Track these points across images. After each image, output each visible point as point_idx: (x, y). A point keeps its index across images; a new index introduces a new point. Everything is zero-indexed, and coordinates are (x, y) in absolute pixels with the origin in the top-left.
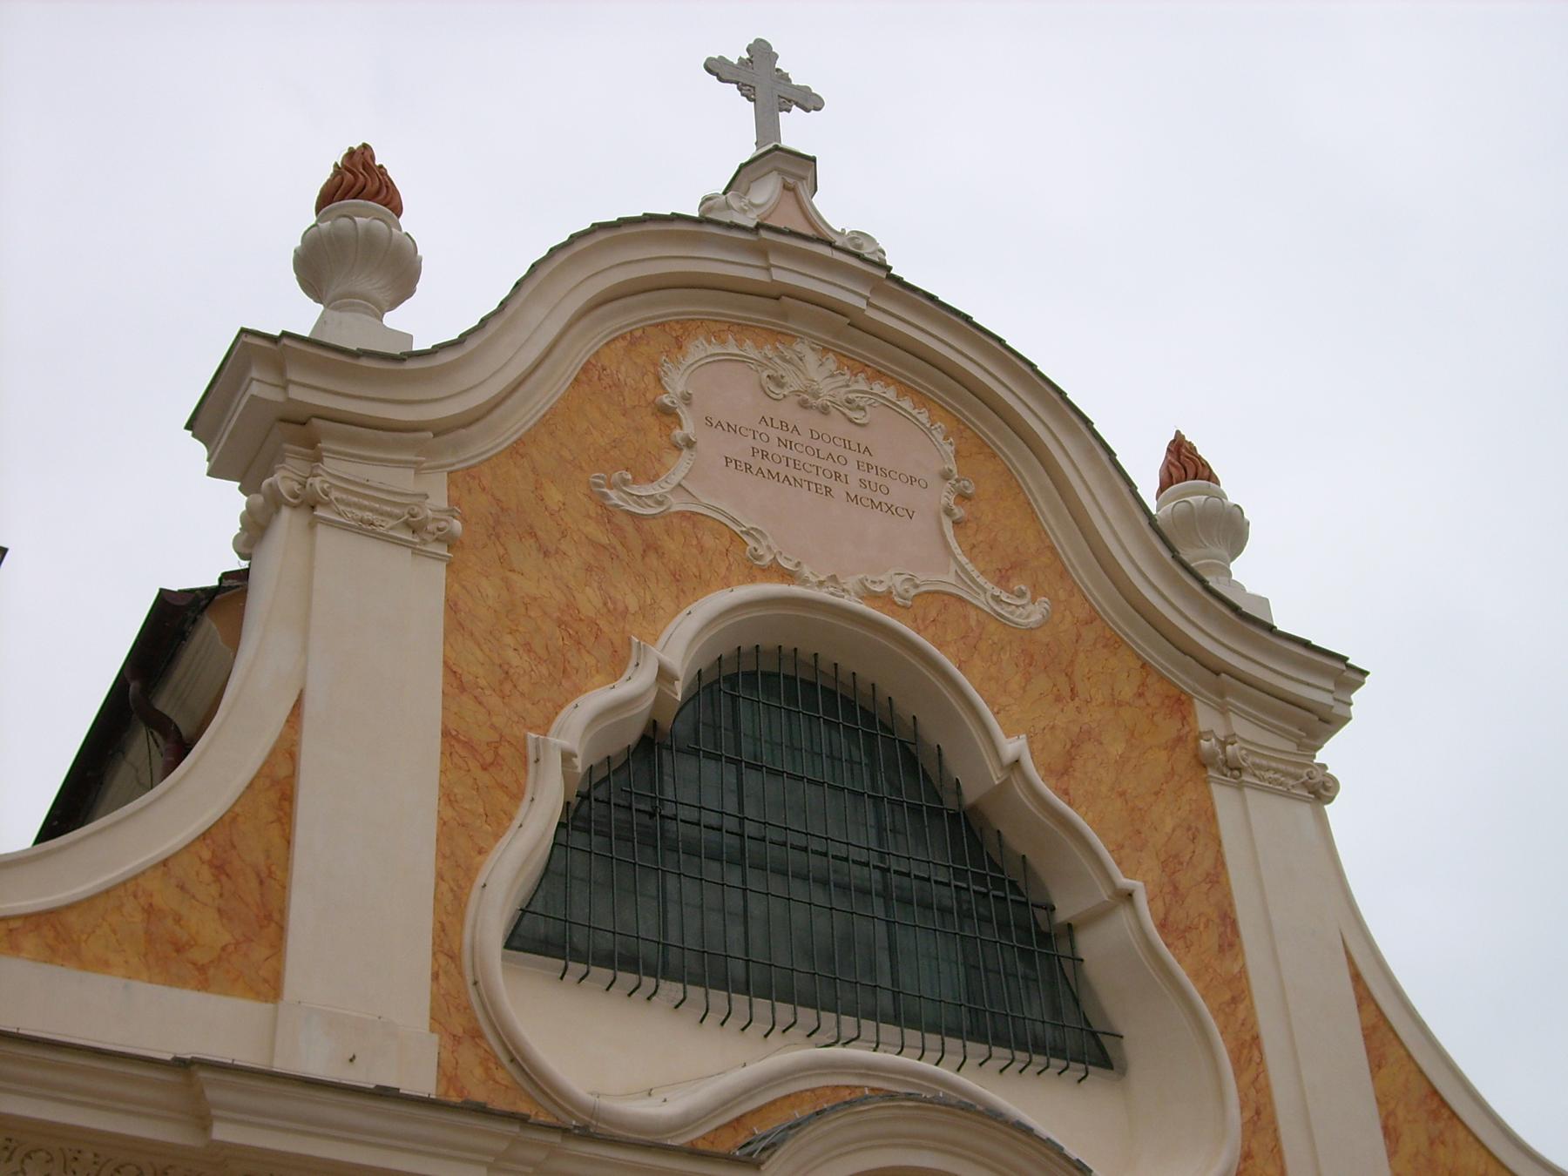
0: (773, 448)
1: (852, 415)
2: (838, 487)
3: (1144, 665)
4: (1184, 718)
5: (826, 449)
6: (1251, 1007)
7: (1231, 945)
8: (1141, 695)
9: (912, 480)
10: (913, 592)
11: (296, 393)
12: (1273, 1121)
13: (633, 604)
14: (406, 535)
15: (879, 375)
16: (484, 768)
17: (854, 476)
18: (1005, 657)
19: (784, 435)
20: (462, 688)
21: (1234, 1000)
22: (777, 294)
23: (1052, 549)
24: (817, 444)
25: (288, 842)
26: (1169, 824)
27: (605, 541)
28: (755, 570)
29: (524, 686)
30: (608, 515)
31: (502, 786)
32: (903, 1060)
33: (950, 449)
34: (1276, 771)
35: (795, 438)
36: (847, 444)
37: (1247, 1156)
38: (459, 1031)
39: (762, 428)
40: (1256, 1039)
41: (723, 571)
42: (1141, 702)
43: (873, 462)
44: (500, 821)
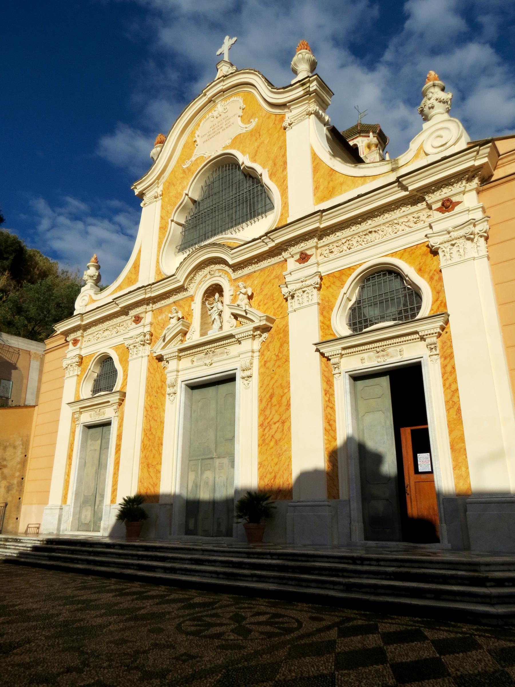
5: (219, 124)
10: (230, 141)
14: (155, 200)
21: (284, 181)
22: (210, 101)
26: (276, 150)
30: (184, 172)
33: (241, 101)
36: (224, 119)
37: (282, 215)
40: (287, 187)
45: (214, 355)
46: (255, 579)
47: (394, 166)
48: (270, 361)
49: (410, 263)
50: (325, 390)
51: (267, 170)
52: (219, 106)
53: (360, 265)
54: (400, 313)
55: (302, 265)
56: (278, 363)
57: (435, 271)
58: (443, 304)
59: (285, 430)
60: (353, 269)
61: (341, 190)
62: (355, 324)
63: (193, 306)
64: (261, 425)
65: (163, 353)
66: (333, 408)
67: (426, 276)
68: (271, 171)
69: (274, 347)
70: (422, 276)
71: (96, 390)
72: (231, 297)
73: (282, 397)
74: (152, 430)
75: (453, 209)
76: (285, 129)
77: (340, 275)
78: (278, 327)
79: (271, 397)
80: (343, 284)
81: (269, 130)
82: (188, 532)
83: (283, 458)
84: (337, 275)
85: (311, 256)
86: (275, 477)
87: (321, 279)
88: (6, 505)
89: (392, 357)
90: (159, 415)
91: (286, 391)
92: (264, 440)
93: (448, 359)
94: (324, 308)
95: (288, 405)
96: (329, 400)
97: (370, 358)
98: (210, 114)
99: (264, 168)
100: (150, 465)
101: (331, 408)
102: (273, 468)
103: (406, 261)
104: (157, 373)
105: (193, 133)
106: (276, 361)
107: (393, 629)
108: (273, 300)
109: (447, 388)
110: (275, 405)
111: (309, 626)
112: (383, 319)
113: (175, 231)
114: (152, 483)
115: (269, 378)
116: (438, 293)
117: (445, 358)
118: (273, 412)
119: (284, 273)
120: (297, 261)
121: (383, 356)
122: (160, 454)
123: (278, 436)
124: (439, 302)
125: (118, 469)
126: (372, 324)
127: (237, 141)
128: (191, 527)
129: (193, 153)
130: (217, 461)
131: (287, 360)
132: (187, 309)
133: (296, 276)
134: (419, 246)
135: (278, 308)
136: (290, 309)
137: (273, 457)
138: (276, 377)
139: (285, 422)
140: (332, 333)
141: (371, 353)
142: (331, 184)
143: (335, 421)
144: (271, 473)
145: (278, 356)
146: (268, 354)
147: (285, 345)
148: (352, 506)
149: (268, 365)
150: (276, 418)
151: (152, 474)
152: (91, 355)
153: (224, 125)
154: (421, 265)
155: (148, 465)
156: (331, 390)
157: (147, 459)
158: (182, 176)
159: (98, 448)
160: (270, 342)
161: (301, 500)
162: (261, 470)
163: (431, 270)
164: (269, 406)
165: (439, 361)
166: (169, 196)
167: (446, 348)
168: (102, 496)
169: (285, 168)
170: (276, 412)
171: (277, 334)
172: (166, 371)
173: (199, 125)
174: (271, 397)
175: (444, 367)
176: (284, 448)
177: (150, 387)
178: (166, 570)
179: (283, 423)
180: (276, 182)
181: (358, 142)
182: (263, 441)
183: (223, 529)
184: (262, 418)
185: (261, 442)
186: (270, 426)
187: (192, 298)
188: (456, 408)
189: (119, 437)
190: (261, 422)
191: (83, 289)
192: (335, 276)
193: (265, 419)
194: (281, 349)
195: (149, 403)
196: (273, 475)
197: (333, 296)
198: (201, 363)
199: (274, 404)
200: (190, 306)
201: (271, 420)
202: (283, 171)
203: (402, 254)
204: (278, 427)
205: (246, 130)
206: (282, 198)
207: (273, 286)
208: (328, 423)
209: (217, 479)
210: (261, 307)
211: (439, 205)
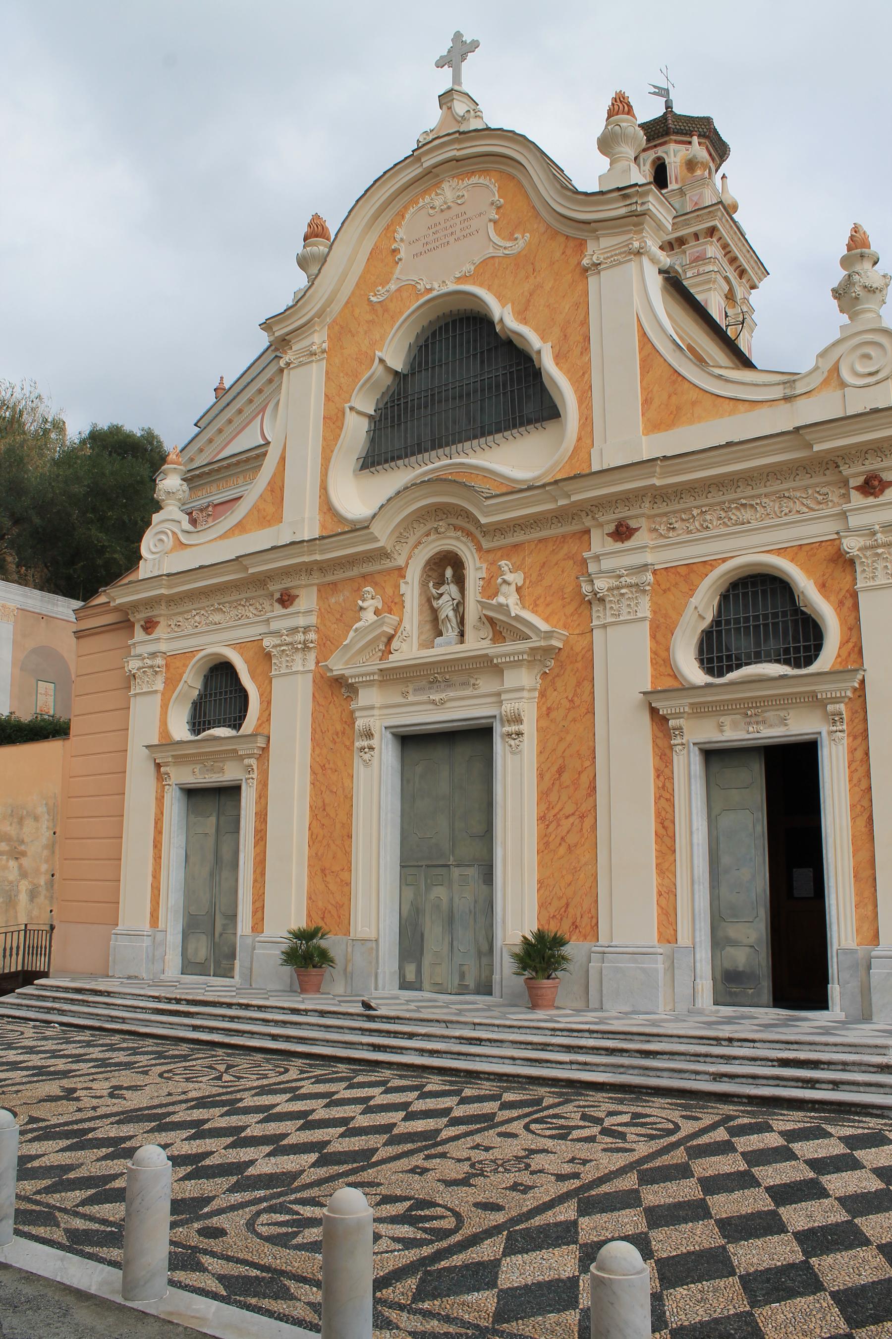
1: (459, 202)
2: (451, 239)
3: (567, 236)
5: (448, 224)
10: (473, 268)
11: (277, 334)
15: (473, 173)
19: (434, 230)
21: (584, 374)
26: (567, 307)
28: (419, 295)
32: (453, 461)
33: (495, 190)
34: (616, 255)
36: (457, 216)
37: (579, 439)
45: (449, 686)
46: (574, 1067)
49: (809, 572)
51: (550, 344)
52: (445, 185)
53: (724, 560)
54: (787, 651)
55: (619, 546)
58: (856, 649)
59: (584, 830)
60: (711, 565)
62: (710, 660)
63: (403, 588)
64: (542, 818)
65: (347, 673)
66: (671, 801)
67: (832, 598)
68: (557, 348)
69: (566, 685)
70: (827, 597)
71: (199, 723)
72: (481, 583)
73: (580, 773)
75: (882, 491)
76: (586, 270)
77: (687, 575)
78: (572, 649)
79: (560, 771)
80: (692, 591)
81: (552, 264)
82: (404, 985)
83: (582, 875)
85: (637, 530)
86: (567, 905)
87: (655, 572)
88: (52, 928)
89: (771, 726)
91: (587, 763)
92: (547, 844)
94: (658, 627)
95: (593, 789)
96: (664, 786)
97: (735, 725)
98: (427, 199)
99: (543, 338)
100: (327, 872)
102: (563, 890)
103: (802, 567)
105: (389, 231)
106: (569, 709)
107: (790, 1126)
109: (855, 785)
110: (567, 787)
111: (688, 1127)
112: (758, 658)
113: (356, 430)
114: (334, 903)
116: (850, 629)
117: (855, 738)
118: (564, 797)
119: (586, 555)
120: (608, 535)
121: (757, 723)
122: (348, 854)
123: (571, 839)
124: (850, 645)
125: (263, 874)
126: (739, 666)
127: (486, 270)
128: (411, 976)
129: (392, 273)
130: (456, 872)
131: (591, 711)
132: (389, 591)
133: (607, 564)
134: (823, 544)
135: (572, 615)
136: (595, 623)
137: (564, 872)
138: (569, 738)
139: (587, 815)
140: (672, 674)
141: (738, 716)
142: (674, 398)
144: (560, 898)
145: (572, 701)
146: (553, 697)
148: (698, 957)
149: (553, 715)
150: (569, 808)
151: (332, 887)
152: (189, 655)
154: (825, 577)
155: (323, 871)
156: (667, 771)
157: (320, 860)
158: (369, 317)
159: (212, 831)
161: (613, 944)
162: (542, 892)
164: (556, 787)
165: (845, 741)
167: (856, 721)
168: (232, 917)
169: (586, 349)
171: (571, 663)
172: (353, 706)
173: (403, 217)
174: (560, 771)
175: (852, 751)
177: (318, 730)
178: (422, 1051)
179: (582, 817)
180: (570, 373)
181: (666, 153)
182: (545, 845)
183: (470, 981)
184: (544, 807)
186: (558, 821)
187: (401, 572)
188: (866, 816)
189: (262, 816)
190: (542, 814)
191: (156, 518)
192: (679, 574)
193: (548, 809)
194: (579, 691)
196: (564, 901)
198: (424, 698)
199: (565, 785)
200: (397, 587)
201: (561, 810)
202: (582, 353)
203: (795, 552)
205: (507, 252)
206: (579, 407)
207: (563, 571)
208: (662, 823)
209: (456, 899)
210: (540, 609)
211: (860, 481)
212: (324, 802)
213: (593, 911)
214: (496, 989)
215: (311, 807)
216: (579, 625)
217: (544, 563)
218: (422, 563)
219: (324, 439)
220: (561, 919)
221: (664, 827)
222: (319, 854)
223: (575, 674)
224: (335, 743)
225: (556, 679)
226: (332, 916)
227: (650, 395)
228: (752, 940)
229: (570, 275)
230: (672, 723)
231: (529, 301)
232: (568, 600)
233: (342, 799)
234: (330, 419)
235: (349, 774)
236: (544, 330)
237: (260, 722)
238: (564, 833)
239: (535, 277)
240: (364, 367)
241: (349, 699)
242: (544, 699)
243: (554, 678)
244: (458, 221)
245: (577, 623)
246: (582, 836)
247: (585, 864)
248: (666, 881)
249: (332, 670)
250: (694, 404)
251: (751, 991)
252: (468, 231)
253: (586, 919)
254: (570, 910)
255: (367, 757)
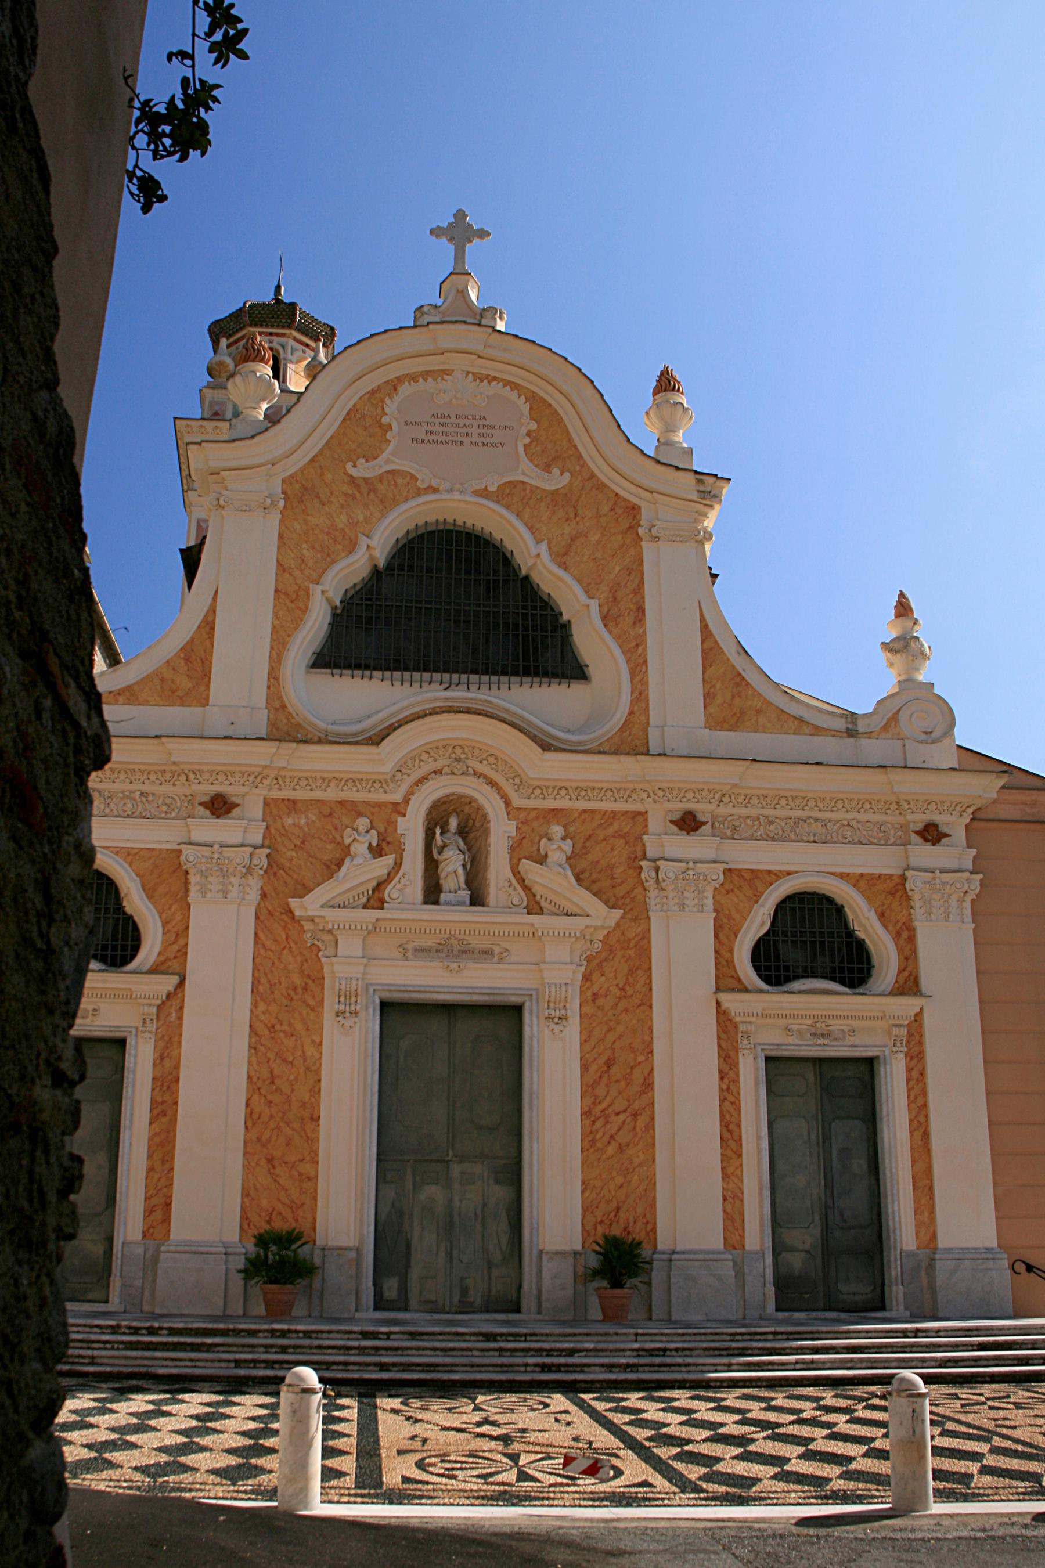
0: (437, 428)
2: (466, 441)
4: (635, 517)
5: (462, 422)
6: (645, 649)
7: (640, 621)
8: (612, 510)
9: (505, 428)
12: (647, 696)
13: (361, 518)
16: (292, 602)
17: (475, 431)
18: (543, 504)
19: (442, 421)
20: (284, 570)
21: (637, 646)
23: (575, 446)
24: (458, 421)
25: (212, 645)
26: (617, 569)
27: (350, 492)
29: (310, 564)
30: (353, 480)
31: (299, 608)
35: (447, 421)
36: (474, 418)
37: (631, 713)
38: (277, 706)
39: (432, 420)
40: (645, 662)
41: (405, 493)
42: (613, 513)
43: (486, 423)
44: (298, 622)
47: (850, 726)
48: (606, 996)
50: (720, 1072)
54: (842, 970)
56: (622, 1005)
57: (904, 924)
58: (912, 978)
59: (638, 1129)
61: (757, 721)
64: (586, 1114)
68: (605, 609)
69: (616, 971)
73: (632, 1068)
74: (278, 1082)
78: (623, 934)
79: (609, 1064)
83: (636, 1177)
84: (748, 876)
86: (618, 1209)
89: (836, 1039)
90: (300, 1053)
91: (641, 1058)
92: (593, 1142)
93: (916, 1060)
95: (648, 1085)
96: (728, 1089)
100: (276, 1163)
101: (732, 1103)
102: (613, 1193)
104: (286, 952)
106: (620, 998)
108: (613, 878)
110: (617, 1081)
114: (287, 1201)
115: (605, 1028)
116: (907, 959)
117: (912, 1058)
118: (613, 1093)
120: (671, 822)
122: (312, 1141)
123: (623, 1137)
124: (906, 973)
131: (646, 1003)
135: (623, 897)
137: (614, 1173)
138: (620, 1029)
142: (737, 701)
143: (739, 1126)
144: (609, 1202)
145: (622, 989)
146: (599, 982)
147: (640, 973)
149: (601, 1001)
150: (620, 1104)
153: (475, 431)
155: (270, 1160)
156: (732, 1074)
157: (264, 1146)
160: (606, 959)
163: (898, 921)
164: (604, 1081)
165: (904, 1061)
166: (306, 521)
170: (620, 1093)
171: (622, 948)
173: (395, 388)
174: (609, 1064)
175: (909, 1070)
176: (636, 1161)
179: (635, 1115)
182: (590, 1142)
184: (589, 1101)
185: (587, 1145)
186: (607, 1117)
187: (399, 809)
188: (921, 1130)
190: (587, 1109)
193: (594, 1103)
195: (263, 1018)
196: (614, 1204)
197: (738, 911)
199: (614, 1079)
200: (391, 823)
202: (635, 623)
203: (857, 880)
204: (624, 1122)
206: (632, 679)
207: (612, 849)
208: (727, 1127)
209: (457, 1203)
211: (920, 827)
212: (271, 1072)
213: (648, 1216)
214: (528, 1302)
215: (249, 1077)
216: (631, 909)
217: (590, 836)
218: (428, 803)
219: (276, 616)
220: (611, 1224)
221: (729, 1131)
222: (264, 1138)
223: (626, 961)
224: (292, 999)
225: (605, 964)
226: (284, 1218)
227: (712, 690)
228: (807, 1246)
229: (620, 537)
230: (741, 1028)
231: (570, 546)
232: (619, 881)
233: (302, 1071)
234: (286, 594)
235: (313, 1042)
236: (589, 584)
237: (162, 958)
238: (614, 1131)
239: (578, 523)
240: (340, 547)
241: (314, 948)
242: (588, 984)
243: (601, 962)
244: (475, 423)
245: (629, 907)
246: (635, 1135)
247: (640, 1165)
248: (731, 1186)
249: (306, 909)
250: (758, 711)
251: (807, 1296)
252: (488, 440)
253: (639, 1224)
254: (622, 1215)
255: (348, 1023)
